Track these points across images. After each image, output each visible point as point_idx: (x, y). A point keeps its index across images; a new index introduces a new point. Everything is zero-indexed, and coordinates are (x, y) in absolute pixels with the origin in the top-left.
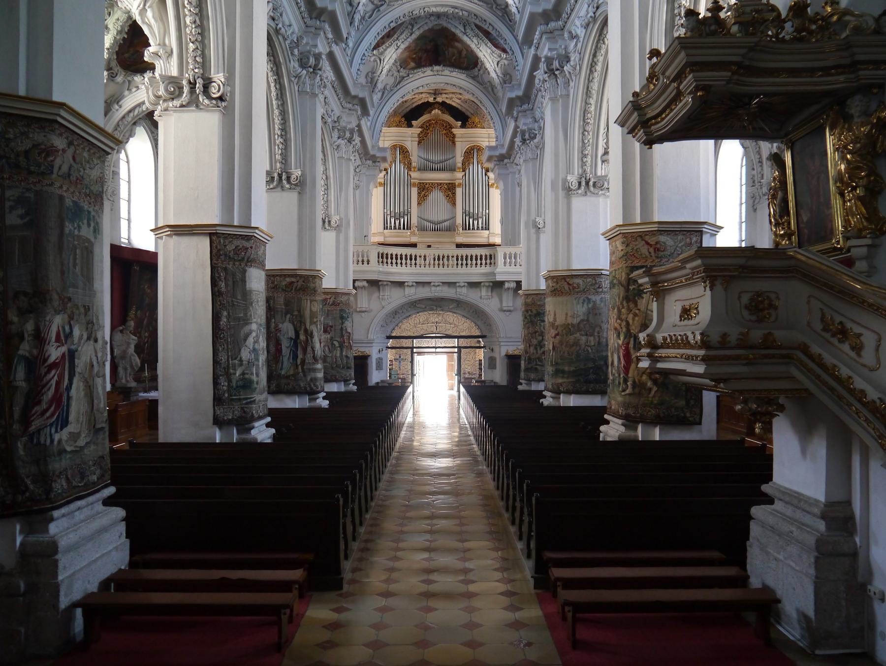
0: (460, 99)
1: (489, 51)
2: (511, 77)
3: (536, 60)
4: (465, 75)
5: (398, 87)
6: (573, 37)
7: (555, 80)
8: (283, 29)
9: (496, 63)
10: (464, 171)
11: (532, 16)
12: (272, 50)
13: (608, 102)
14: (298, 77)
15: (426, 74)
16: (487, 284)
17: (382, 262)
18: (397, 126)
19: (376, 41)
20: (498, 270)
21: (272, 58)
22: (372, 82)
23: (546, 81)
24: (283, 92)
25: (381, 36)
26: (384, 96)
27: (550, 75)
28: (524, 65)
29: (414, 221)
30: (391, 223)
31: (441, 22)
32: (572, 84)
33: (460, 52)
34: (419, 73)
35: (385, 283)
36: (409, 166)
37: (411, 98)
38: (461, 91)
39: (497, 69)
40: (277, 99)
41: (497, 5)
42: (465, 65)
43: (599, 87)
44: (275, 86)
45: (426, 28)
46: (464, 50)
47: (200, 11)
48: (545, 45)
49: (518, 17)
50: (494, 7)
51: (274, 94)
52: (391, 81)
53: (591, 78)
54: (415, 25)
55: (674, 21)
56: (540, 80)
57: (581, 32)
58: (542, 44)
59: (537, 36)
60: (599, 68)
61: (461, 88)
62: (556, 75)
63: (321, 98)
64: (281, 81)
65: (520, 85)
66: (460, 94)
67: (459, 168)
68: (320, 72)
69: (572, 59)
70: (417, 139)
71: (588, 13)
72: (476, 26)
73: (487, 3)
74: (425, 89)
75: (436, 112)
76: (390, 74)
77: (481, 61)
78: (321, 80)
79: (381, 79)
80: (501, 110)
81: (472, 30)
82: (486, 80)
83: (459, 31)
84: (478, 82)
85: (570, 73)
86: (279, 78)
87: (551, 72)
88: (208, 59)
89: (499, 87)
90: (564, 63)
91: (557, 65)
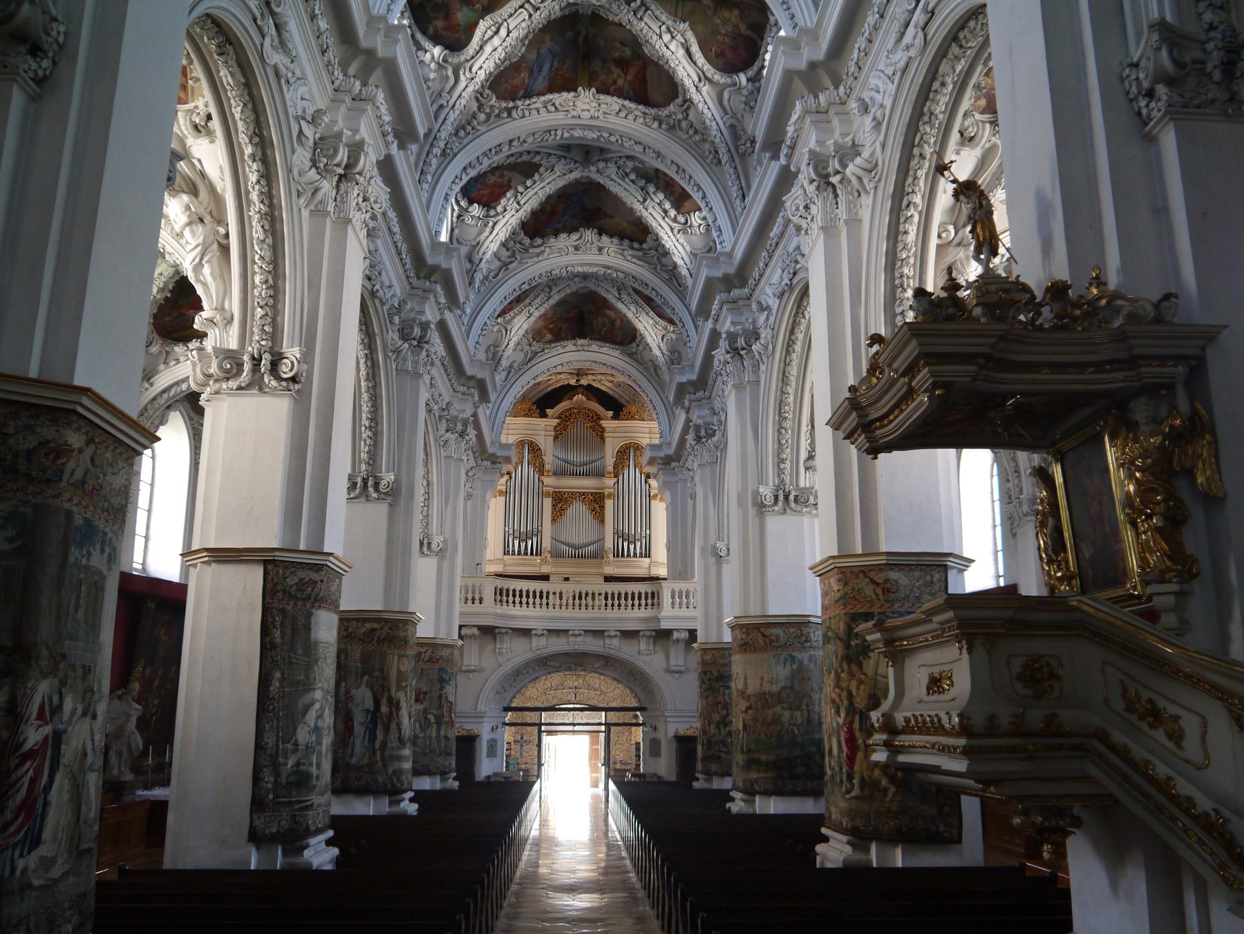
0: (612, 382)
1: (651, 322)
2: (680, 354)
3: (715, 336)
5: (529, 365)
6: (763, 308)
7: (740, 362)
8: (381, 291)
9: (660, 337)
10: (616, 476)
11: (709, 282)
12: (364, 317)
14: (397, 351)
15: (567, 349)
16: (648, 633)
17: (501, 601)
18: (526, 415)
20: (663, 614)
21: (364, 327)
22: (494, 357)
24: (376, 370)
25: (508, 301)
29: (547, 543)
30: (513, 546)
32: (763, 368)
33: (612, 323)
34: (558, 348)
35: (504, 631)
36: (541, 470)
38: (614, 372)
40: (367, 379)
41: (663, 266)
43: (798, 372)
44: (366, 362)
45: (568, 291)
47: (274, 268)
48: (726, 317)
49: (690, 281)
50: (658, 268)
51: (363, 372)
52: (520, 357)
53: (788, 361)
55: (894, 294)
57: (773, 303)
58: (722, 316)
60: (798, 347)
62: (741, 356)
63: (427, 378)
65: (693, 366)
67: (609, 473)
68: (427, 346)
69: (763, 336)
70: (553, 433)
71: (782, 280)
72: (635, 290)
73: (650, 264)
74: (566, 369)
76: (519, 348)
79: (506, 354)
82: (647, 358)
83: (611, 297)
84: (637, 361)
85: (759, 353)
86: (371, 353)
87: (734, 351)
88: (280, 328)
89: (664, 368)
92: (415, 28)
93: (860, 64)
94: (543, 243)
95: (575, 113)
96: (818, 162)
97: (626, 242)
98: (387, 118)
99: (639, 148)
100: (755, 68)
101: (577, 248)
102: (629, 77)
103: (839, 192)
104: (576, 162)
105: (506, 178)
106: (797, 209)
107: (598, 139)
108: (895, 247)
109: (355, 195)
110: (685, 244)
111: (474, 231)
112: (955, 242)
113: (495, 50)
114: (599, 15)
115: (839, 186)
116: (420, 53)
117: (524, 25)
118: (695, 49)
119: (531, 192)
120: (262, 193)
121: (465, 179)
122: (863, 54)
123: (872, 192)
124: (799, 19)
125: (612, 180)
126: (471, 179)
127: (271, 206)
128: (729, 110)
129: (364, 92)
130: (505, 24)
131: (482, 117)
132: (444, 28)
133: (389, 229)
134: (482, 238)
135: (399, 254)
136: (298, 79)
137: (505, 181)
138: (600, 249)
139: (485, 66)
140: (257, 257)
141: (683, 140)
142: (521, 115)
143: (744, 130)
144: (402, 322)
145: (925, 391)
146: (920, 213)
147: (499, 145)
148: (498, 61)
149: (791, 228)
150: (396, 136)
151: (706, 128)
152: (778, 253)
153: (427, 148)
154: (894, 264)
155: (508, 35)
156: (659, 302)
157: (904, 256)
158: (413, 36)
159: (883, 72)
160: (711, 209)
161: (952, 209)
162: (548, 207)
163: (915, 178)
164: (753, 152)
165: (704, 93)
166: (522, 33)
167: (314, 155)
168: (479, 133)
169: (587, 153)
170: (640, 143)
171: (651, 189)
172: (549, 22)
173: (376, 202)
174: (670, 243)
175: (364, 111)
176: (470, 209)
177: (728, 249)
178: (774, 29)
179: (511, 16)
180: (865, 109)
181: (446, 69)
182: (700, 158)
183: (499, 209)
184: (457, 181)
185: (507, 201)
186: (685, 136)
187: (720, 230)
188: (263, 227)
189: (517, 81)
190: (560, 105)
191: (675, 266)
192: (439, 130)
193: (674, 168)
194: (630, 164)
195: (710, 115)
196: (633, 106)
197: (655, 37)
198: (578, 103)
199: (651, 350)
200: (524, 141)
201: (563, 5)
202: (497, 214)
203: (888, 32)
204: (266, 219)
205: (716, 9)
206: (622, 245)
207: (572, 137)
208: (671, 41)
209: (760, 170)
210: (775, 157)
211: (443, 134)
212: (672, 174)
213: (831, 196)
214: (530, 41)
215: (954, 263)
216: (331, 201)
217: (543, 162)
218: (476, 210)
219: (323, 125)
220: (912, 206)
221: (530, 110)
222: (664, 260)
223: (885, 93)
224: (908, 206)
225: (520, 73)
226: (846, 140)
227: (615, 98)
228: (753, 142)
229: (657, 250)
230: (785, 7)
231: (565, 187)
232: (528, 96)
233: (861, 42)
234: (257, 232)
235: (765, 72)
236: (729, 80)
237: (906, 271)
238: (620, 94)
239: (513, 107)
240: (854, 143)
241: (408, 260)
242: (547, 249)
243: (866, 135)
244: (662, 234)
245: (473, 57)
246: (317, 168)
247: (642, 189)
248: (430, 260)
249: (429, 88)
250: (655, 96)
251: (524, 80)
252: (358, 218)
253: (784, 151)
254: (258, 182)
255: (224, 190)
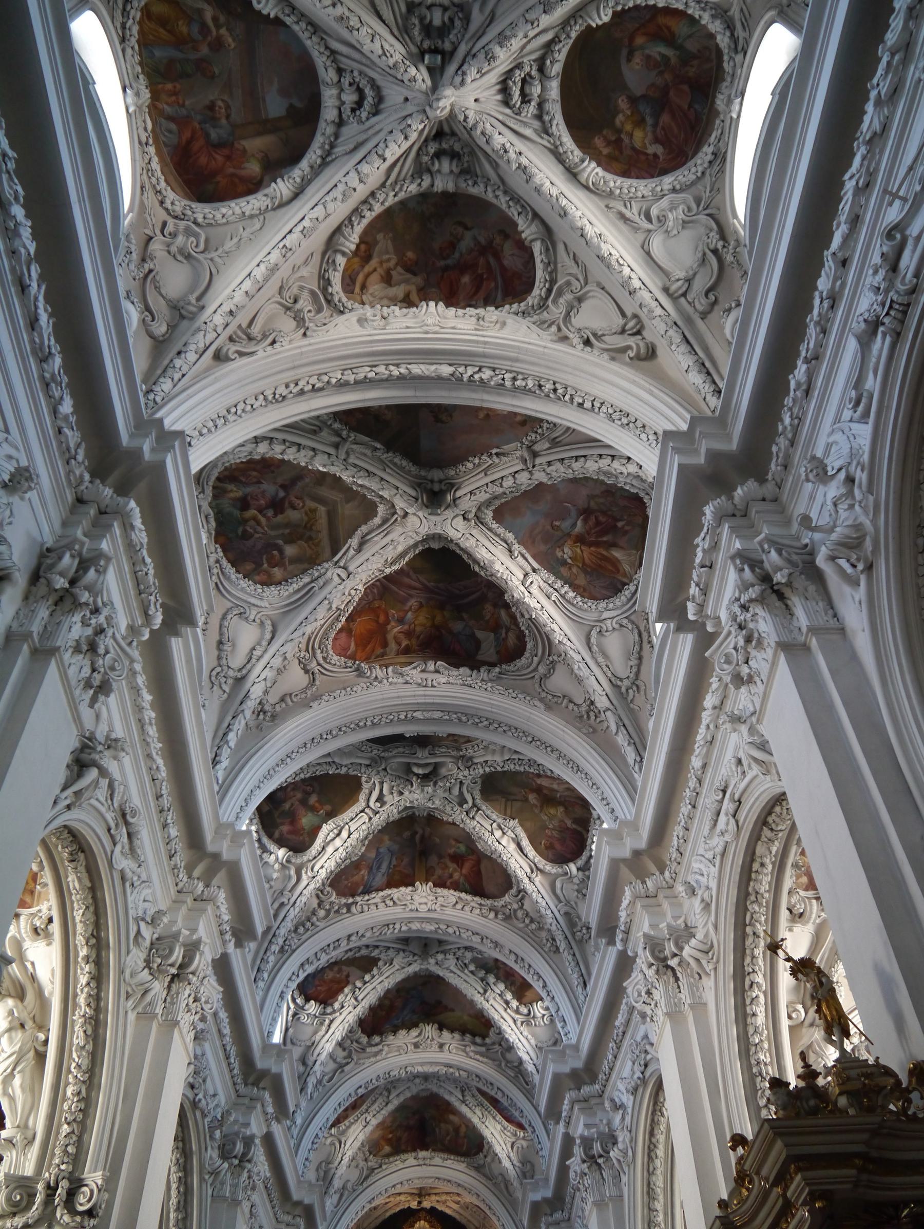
0: (458, 1203)
2: (533, 1166)
3: (568, 1141)
4: (464, 1165)
6: (618, 1107)
7: (598, 1172)
8: (204, 1102)
9: (509, 1145)
11: (557, 1077)
12: (183, 1132)
13: (682, 1207)
14: (215, 1173)
15: (407, 1164)
19: (336, 1116)
21: (180, 1144)
22: (326, 1177)
23: (586, 1174)
24: (189, 1198)
25: (343, 1108)
27: (591, 1165)
28: (551, 1149)
31: (430, 1087)
32: (624, 1179)
33: (457, 1130)
34: (397, 1163)
37: (383, 1202)
38: (460, 1191)
39: (512, 1154)
40: (177, 1210)
41: (508, 1062)
42: (465, 1148)
43: (665, 1183)
44: (178, 1188)
45: (408, 1095)
46: (463, 1126)
47: (90, 1078)
48: (578, 1120)
49: (537, 1078)
50: (503, 1064)
51: (174, 1201)
52: (354, 1175)
53: (651, 1169)
54: (393, 1090)
55: (754, 1084)
56: (576, 1172)
57: (627, 1099)
58: (574, 1118)
59: (566, 1107)
60: (660, 1152)
61: (459, 1185)
62: (599, 1165)
63: (246, 1206)
64: (189, 1180)
65: (547, 1180)
66: (458, 1195)
68: (249, 1166)
69: (620, 1139)
71: (634, 1073)
72: (479, 1090)
73: (494, 1060)
74: (406, 1188)
76: (354, 1164)
77: (488, 1143)
78: (249, 1177)
79: (339, 1172)
80: (521, 1221)
81: (473, 1096)
82: (496, 1172)
83: (454, 1099)
84: (485, 1175)
85: (619, 1161)
86: (186, 1176)
87: (590, 1159)
88: (85, 1149)
89: (516, 1184)
90: (610, 1145)
91: (600, 1149)
92: (262, 832)
93: (682, 850)
94: (382, 1041)
95: (413, 907)
96: (654, 946)
97: (468, 1037)
98: (226, 917)
99: (476, 939)
100: (584, 857)
101: (416, 1046)
102: (464, 871)
103: (679, 975)
104: (414, 955)
105: (345, 973)
106: (640, 995)
107: (436, 932)
108: (746, 1032)
109: (186, 995)
110: (530, 1037)
111: (309, 1030)
112: (807, 1023)
113: (336, 850)
114: (434, 816)
115: (677, 969)
116: (265, 855)
117: (364, 827)
118: (525, 843)
119: (369, 987)
120: (90, 995)
121: (302, 976)
122: (682, 841)
123: (712, 973)
124: (619, 812)
125: (452, 972)
126: (308, 975)
127: (97, 1010)
128: (562, 898)
129: (206, 893)
130: (347, 827)
131: (322, 913)
132: (290, 832)
133: (219, 1031)
134: (318, 1037)
135: (228, 1058)
136: (144, 882)
137: (343, 977)
138: (441, 1046)
139: (326, 865)
140: (74, 1065)
141: (519, 929)
142: (360, 910)
143: (579, 917)
144: (224, 1136)
145: (804, 1204)
146: (765, 993)
147: (338, 940)
148: (339, 861)
149: (636, 1017)
150: (234, 934)
151: (541, 916)
152: (626, 1043)
153: (265, 945)
154: (748, 1050)
155: (349, 837)
156: (506, 1104)
157: (757, 1041)
158: (259, 840)
159: (703, 856)
160: (553, 998)
161: (796, 989)
162: (387, 1002)
163: (753, 957)
164: (590, 938)
165: (537, 883)
166: (362, 835)
167: (149, 955)
168: (318, 929)
169: (426, 945)
170: (477, 934)
171: (491, 979)
172: (388, 824)
173: (207, 1002)
174: (514, 1036)
175: (204, 911)
176: (307, 1007)
177: (574, 1041)
178: (598, 822)
179: (352, 819)
180: (692, 892)
181: (289, 869)
182: (538, 946)
183: (337, 1005)
184: (294, 977)
185: (345, 998)
186: (522, 925)
187: (564, 1021)
188: (85, 1032)
189: (356, 878)
190: (399, 899)
191: (521, 1062)
192: (278, 927)
193: (513, 957)
194: (469, 955)
195: (544, 904)
196: (469, 897)
197: (487, 834)
198: (416, 897)
199: (500, 1162)
200: (363, 936)
201: (400, 808)
202: (334, 1012)
203: (702, 820)
204: (90, 1023)
205: (542, 807)
206: (463, 1040)
207: (410, 930)
208: (502, 837)
209: (598, 956)
210: (611, 942)
211: (283, 931)
212: (511, 962)
213: (672, 980)
214: (370, 842)
215: (810, 1046)
216: (160, 1002)
217: (382, 956)
218: (312, 1007)
219: (162, 925)
220: (755, 986)
221: (368, 905)
222: (508, 1056)
223: (708, 876)
224: (751, 986)
225: (360, 870)
226: (678, 922)
227: (452, 891)
228: (588, 928)
229: (500, 1045)
230: (605, 802)
231: (403, 980)
232: (367, 891)
233: (678, 830)
234: (78, 1037)
235: (592, 861)
236: (560, 870)
237: (762, 1057)
238: (456, 887)
239: (353, 903)
240: (686, 925)
241: (236, 1066)
242: (386, 1048)
243: (697, 917)
244: (505, 1027)
245: (315, 858)
246: (150, 968)
247: (482, 980)
248: (260, 1064)
249: (271, 887)
250: (489, 887)
251: (363, 876)
252: (186, 1020)
253: (619, 936)
254: (88, 984)
255: (51, 993)
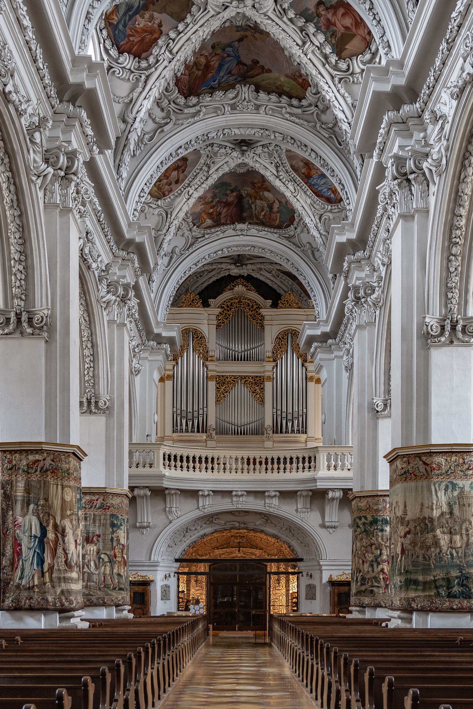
5: (191, 250)
10: (275, 361)
16: (304, 493)
26: (172, 262)
70: (215, 322)
75: (240, 289)
